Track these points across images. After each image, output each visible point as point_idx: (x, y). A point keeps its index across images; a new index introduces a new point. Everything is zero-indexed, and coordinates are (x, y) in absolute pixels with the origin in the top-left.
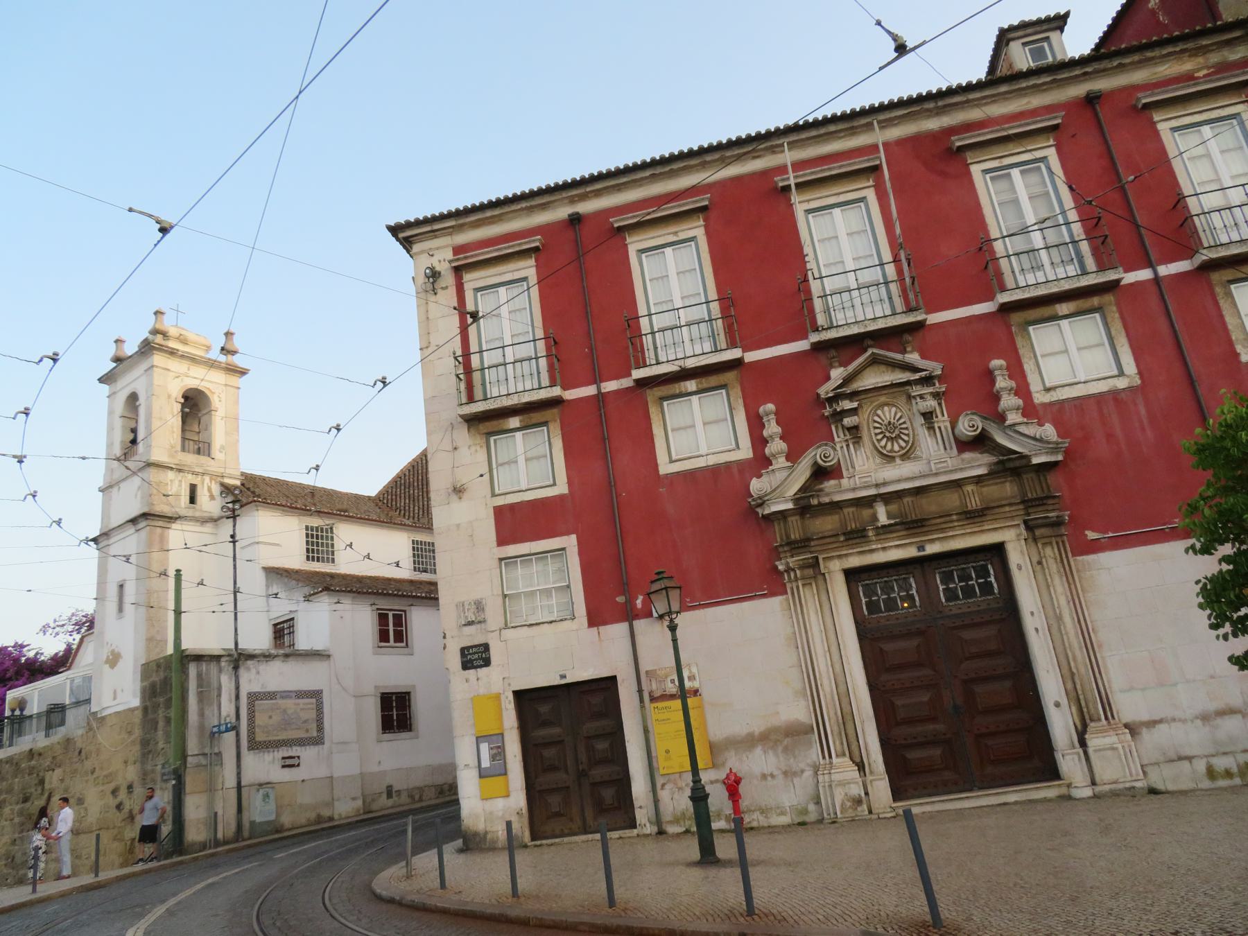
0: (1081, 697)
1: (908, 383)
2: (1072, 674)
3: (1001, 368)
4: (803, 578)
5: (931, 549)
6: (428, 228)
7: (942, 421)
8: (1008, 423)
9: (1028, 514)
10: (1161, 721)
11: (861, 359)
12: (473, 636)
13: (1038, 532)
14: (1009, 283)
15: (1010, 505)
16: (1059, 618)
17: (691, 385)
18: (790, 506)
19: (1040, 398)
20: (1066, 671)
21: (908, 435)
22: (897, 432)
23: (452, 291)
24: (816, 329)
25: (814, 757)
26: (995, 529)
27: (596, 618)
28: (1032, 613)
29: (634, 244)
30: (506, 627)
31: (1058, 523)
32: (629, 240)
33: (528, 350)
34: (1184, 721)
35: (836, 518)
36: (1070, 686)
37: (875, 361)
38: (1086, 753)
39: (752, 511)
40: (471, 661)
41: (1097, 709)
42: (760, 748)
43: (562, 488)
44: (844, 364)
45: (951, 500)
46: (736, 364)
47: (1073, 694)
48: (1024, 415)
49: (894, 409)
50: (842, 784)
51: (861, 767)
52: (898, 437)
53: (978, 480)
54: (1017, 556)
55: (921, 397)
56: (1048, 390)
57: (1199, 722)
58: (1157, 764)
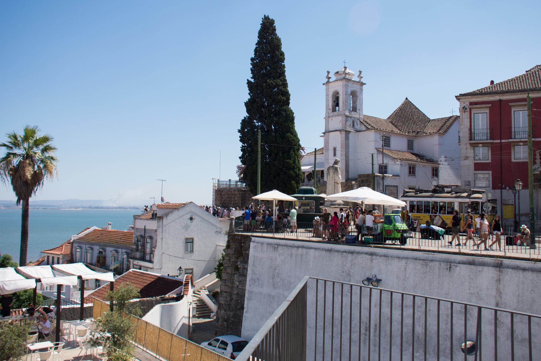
17: (522, 144)
23: (469, 113)
27: (494, 188)
29: (513, 110)
43: (490, 161)
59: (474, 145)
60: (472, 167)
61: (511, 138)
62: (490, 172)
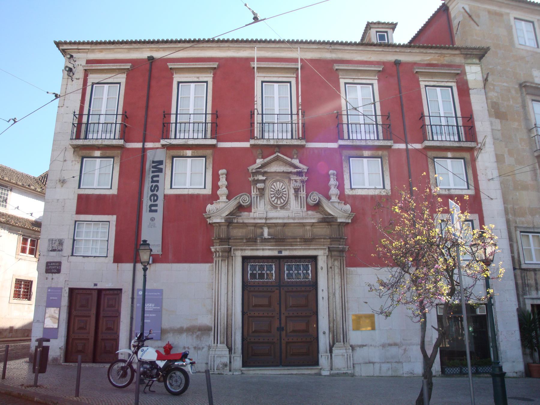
0: (335, 331)
1: (291, 173)
2: (334, 320)
3: (333, 174)
4: (222, 256)
5: (285, 253)
6: (76, 47)
7: (303, 194)
8: (331, 201)
9: (331, 244)
10: (365, 346)
11: (272, 157)
12: (54, 257)
13: (334, 253)
14: (346, 137)
15: (324, 239)
16: (334, 294)
17: (189, 153)
18: (223, 221)
19: (348, 192)
20: (331, 319)
21: (286, 198)
22: (281, 195)
23: (81, 81)
24: (253, 138)
25: (210, 343)
26: (315, 249)
27: (117, 259)
28: (323, 290)
29: (177, 78)
30: (72, 255)
31: (342, 251)
32: (175, 76)
33: (113, 119)
34: (375, 346)
35: (244, 230)
36: (331, 325)
37: (277, 159)
38: (331, 356)
39: (205, 220)
40: (51, 269)
41: (340, 337)
42: (185, 334)
43: (114, 191)
44: (263, 158)
45: (299, 232)
46: (213, 146)
47: (332, 329)
48: (339, 198)
49: (282, 184)
50: (220, 356)
51: (230, 350)
52: (281, 197)
53: (313, 225)
54: (322, 263)
55: (296, 181)
56: (351, 189)
57: (381, 347)
58: (360, 364)
59: (84, 151)
60: (73, 204)
61: (168, 138)
62: (113, 219)
